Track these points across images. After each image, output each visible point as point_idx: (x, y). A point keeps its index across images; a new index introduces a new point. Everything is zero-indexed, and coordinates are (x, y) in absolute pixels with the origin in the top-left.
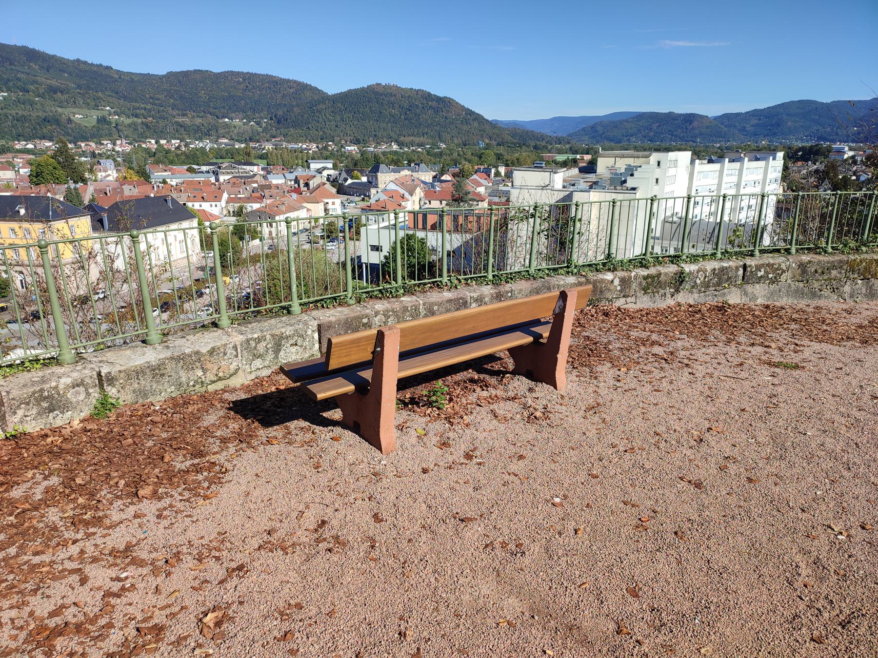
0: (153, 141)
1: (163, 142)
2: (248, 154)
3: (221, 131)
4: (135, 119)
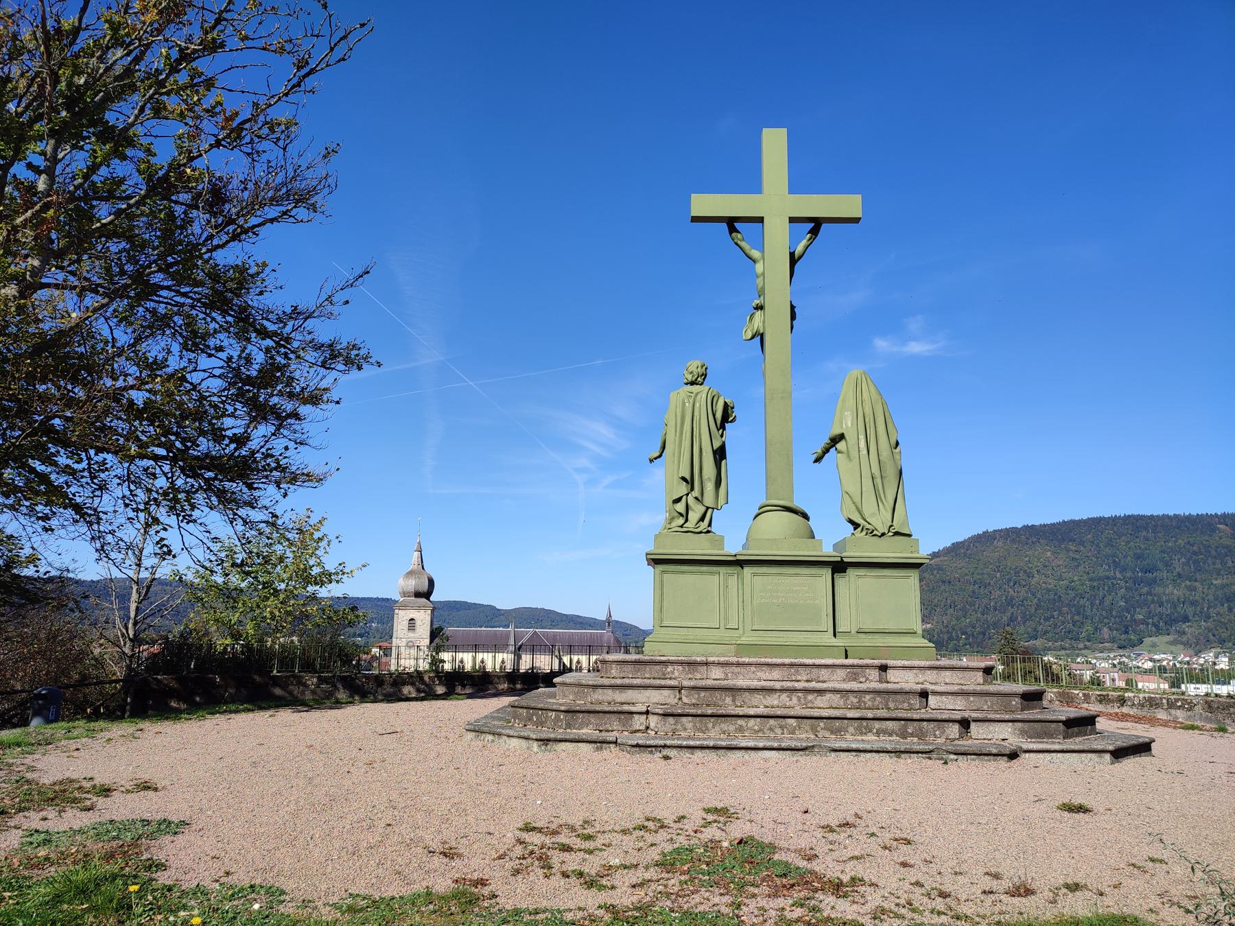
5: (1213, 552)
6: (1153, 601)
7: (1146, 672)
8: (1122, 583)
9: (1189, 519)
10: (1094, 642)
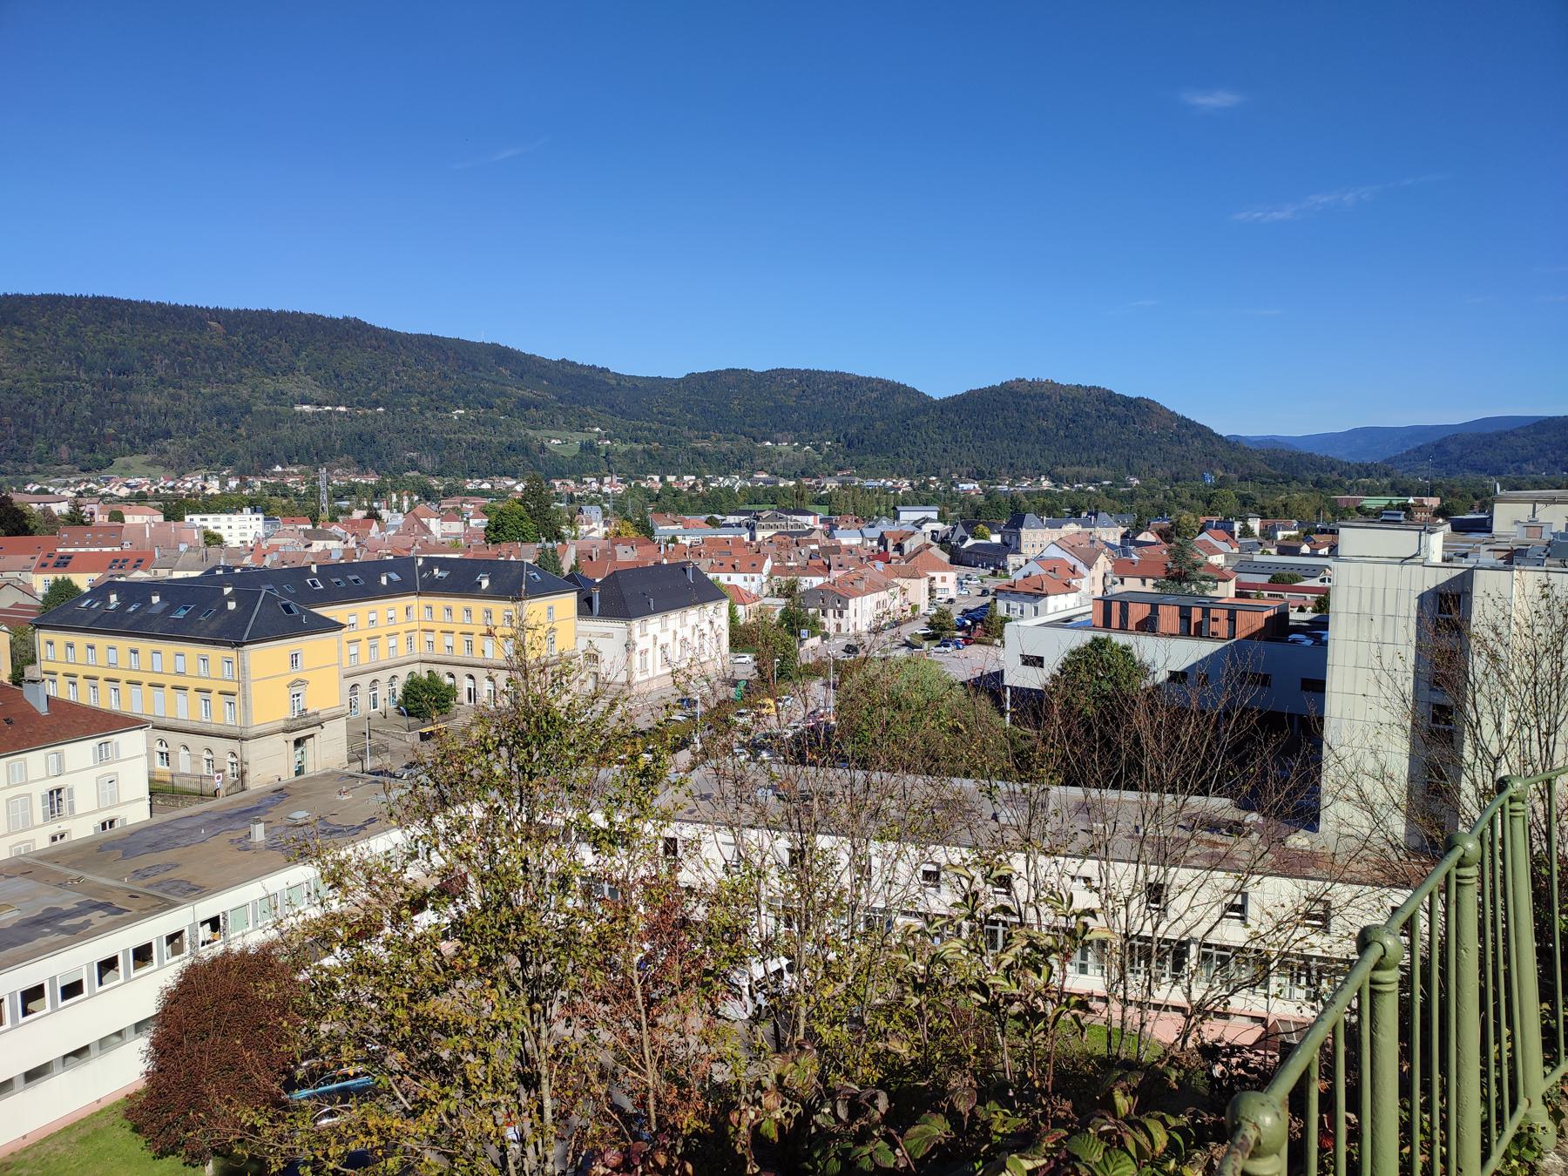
0: (657, 478)
1: (671, 479)
2: (800, 497)
3: (759, 461)
4: (634, 445)
5: (203, 355)
6: (128, 412)
7: (122, 500)
8: (88, 387)
9: (175, 309)
10: (47, 464)
